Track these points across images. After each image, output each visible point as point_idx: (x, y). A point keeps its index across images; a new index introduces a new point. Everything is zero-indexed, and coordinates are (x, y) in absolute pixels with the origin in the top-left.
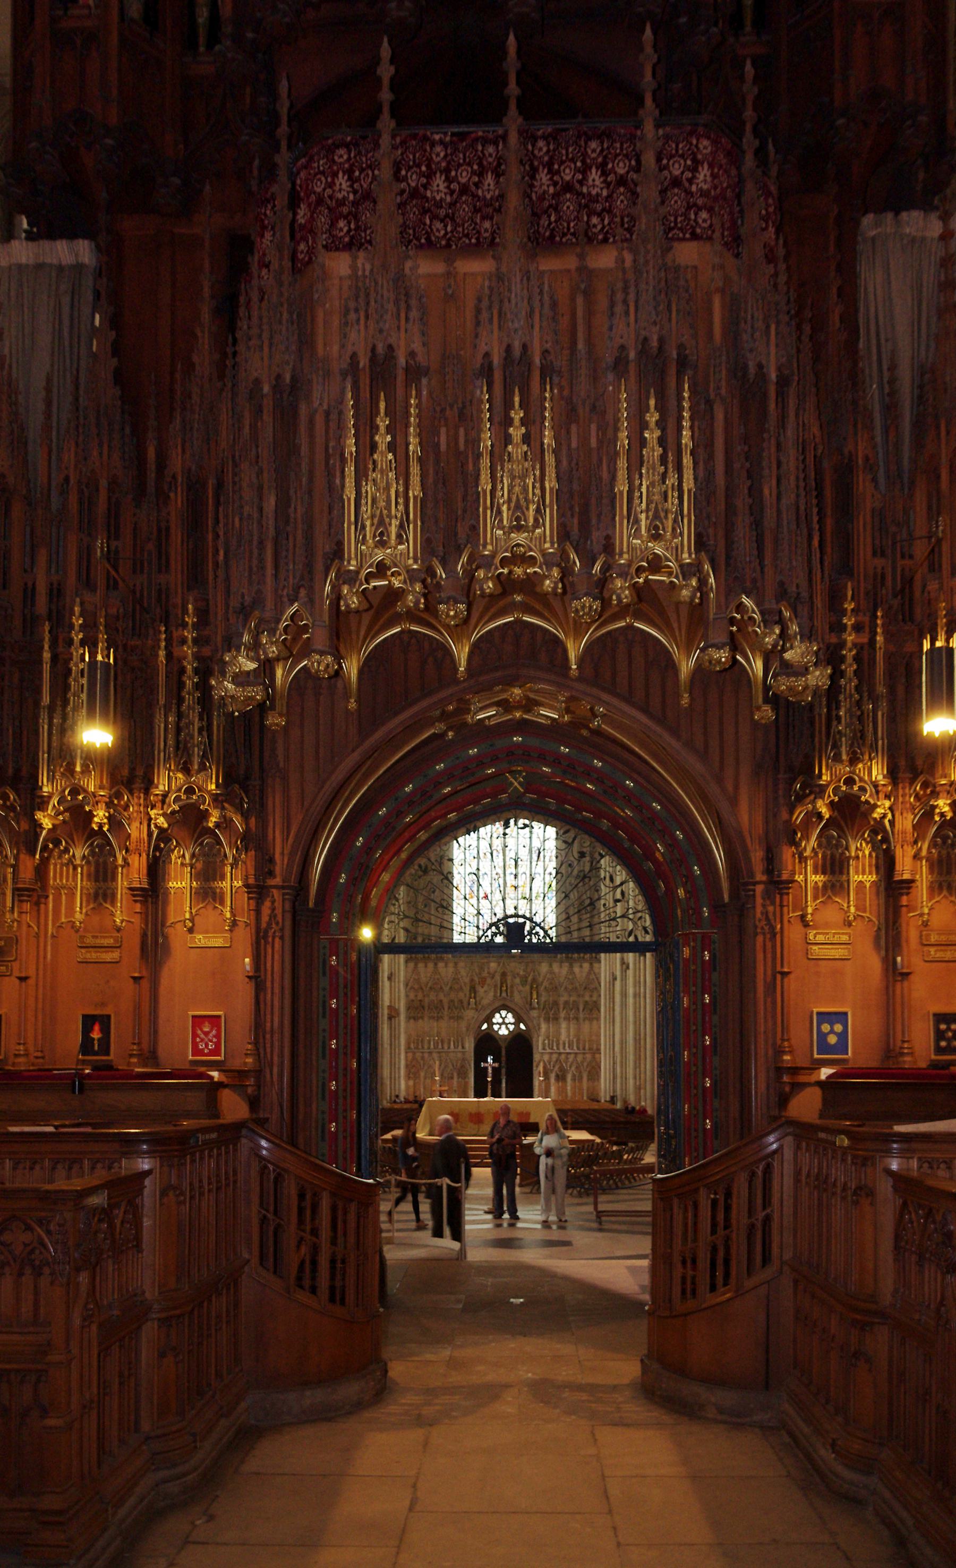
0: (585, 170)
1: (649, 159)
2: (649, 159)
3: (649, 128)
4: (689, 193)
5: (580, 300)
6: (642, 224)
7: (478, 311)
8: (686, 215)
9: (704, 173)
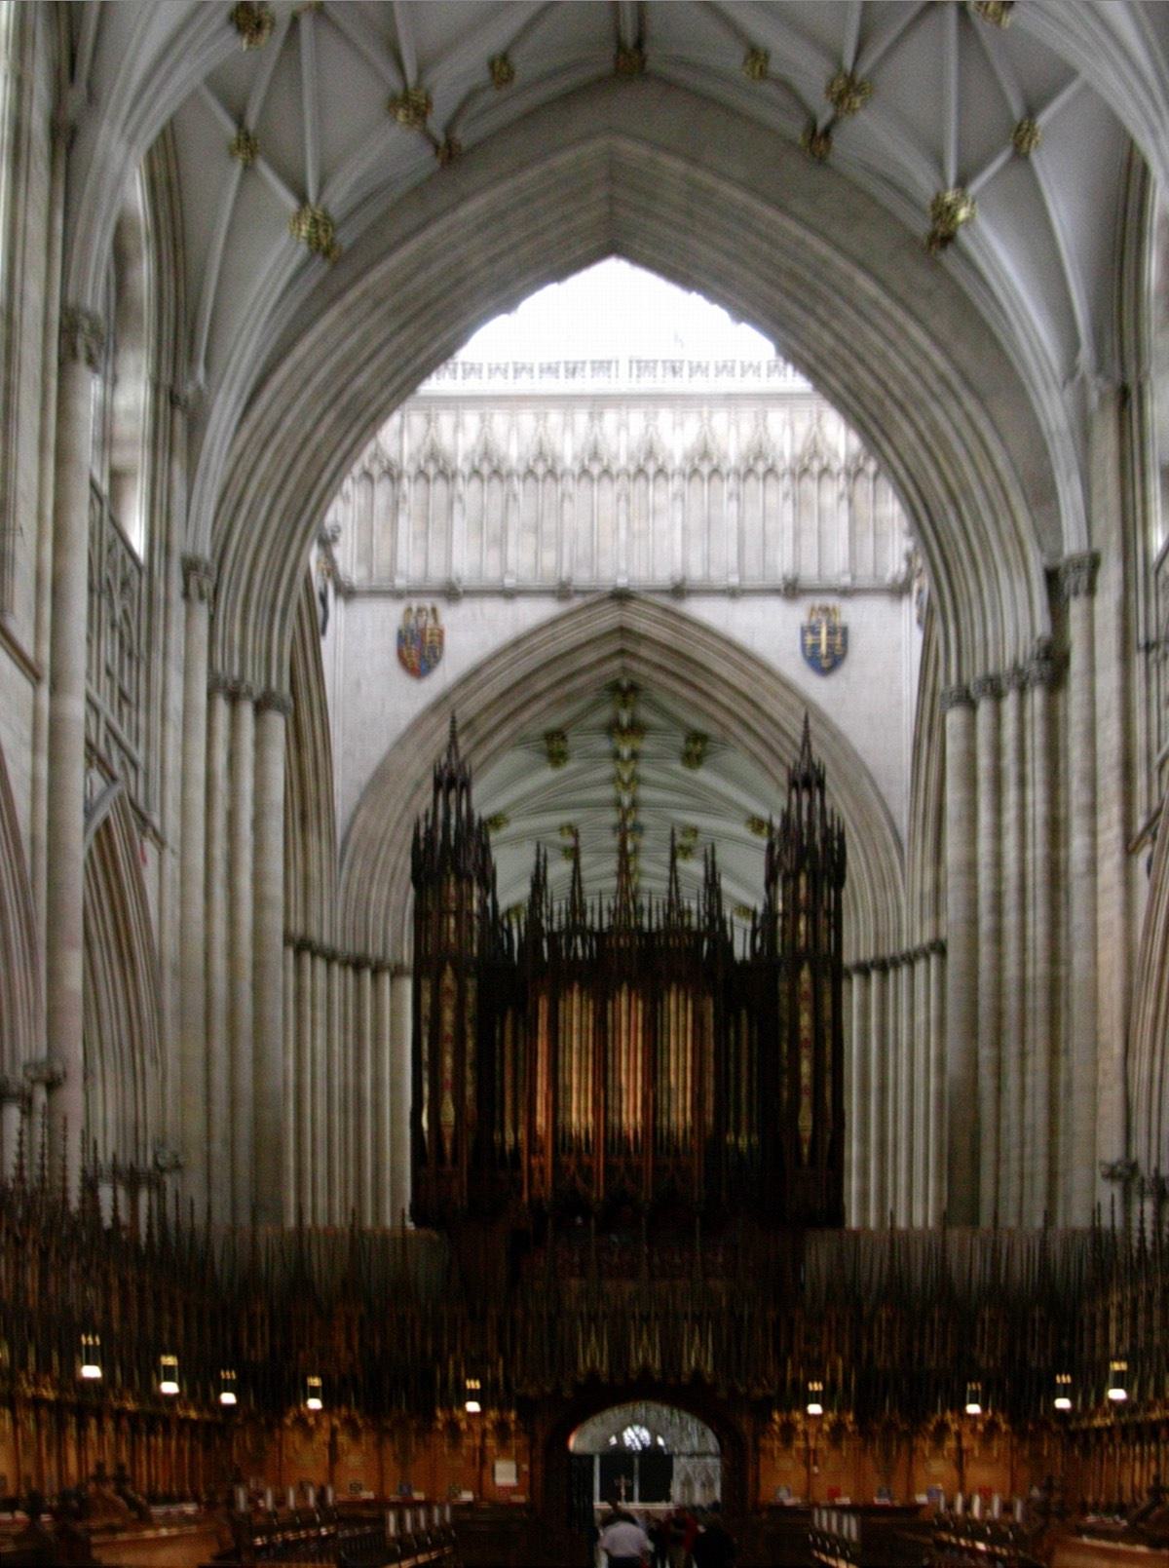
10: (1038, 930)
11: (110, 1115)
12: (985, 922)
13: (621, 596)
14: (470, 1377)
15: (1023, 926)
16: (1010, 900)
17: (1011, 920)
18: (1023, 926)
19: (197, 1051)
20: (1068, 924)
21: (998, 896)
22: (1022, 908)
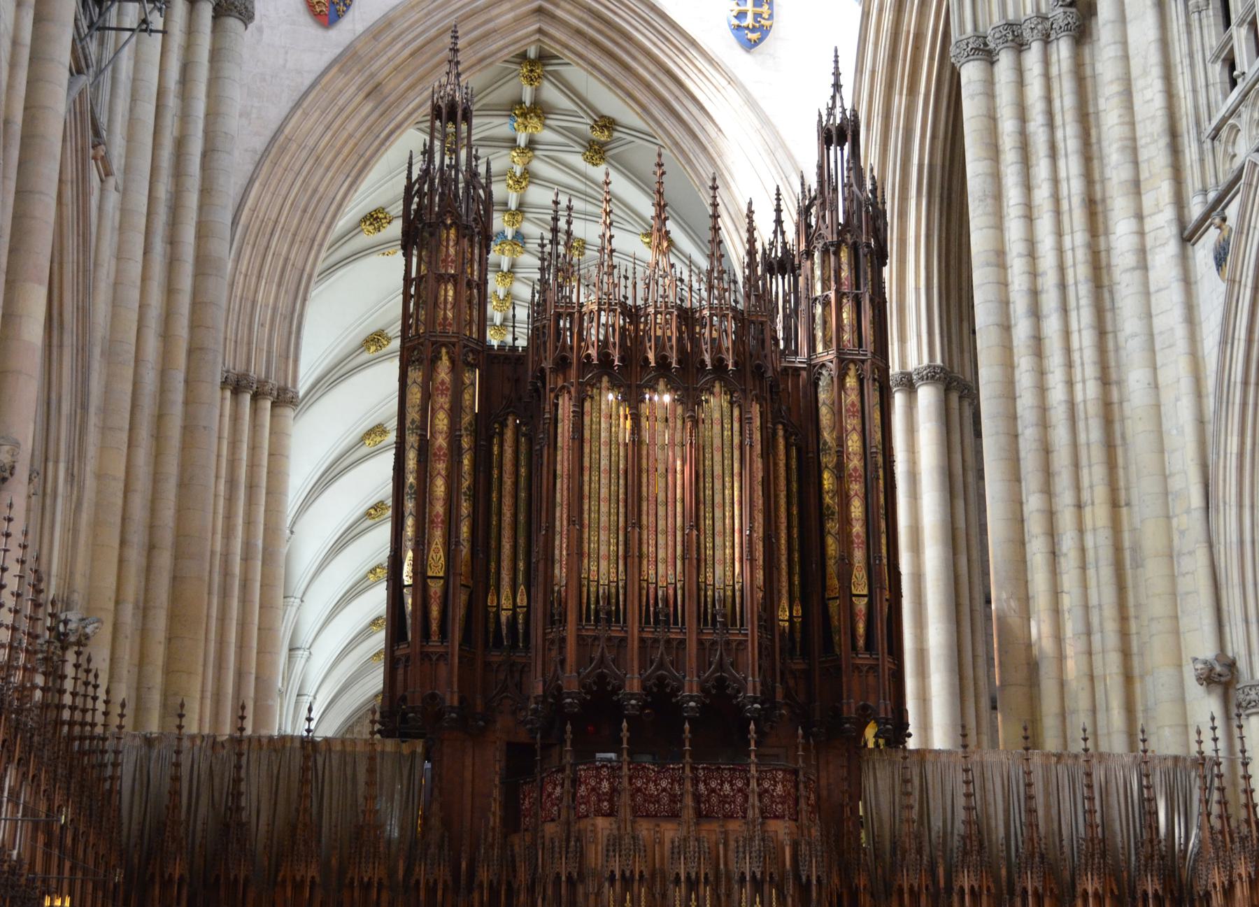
0: (722, 785)
1: (753, 784)
2: (753, 784)
3: (753, 769)
4: (772, 796)
5: (721, 846)
6: (750, 813)
7: (673, 853)
8: (771, 806)
9: (779, 787)
10: (1084, 340)
12: (1022, 330)
15: (1066, 334)
16: (1050, 300)
17: (1052, 326)
18: (1066, 334)
19: (118, 468)
20: (1115, 332)
21: (1034, 294)
22: (1064, 310)
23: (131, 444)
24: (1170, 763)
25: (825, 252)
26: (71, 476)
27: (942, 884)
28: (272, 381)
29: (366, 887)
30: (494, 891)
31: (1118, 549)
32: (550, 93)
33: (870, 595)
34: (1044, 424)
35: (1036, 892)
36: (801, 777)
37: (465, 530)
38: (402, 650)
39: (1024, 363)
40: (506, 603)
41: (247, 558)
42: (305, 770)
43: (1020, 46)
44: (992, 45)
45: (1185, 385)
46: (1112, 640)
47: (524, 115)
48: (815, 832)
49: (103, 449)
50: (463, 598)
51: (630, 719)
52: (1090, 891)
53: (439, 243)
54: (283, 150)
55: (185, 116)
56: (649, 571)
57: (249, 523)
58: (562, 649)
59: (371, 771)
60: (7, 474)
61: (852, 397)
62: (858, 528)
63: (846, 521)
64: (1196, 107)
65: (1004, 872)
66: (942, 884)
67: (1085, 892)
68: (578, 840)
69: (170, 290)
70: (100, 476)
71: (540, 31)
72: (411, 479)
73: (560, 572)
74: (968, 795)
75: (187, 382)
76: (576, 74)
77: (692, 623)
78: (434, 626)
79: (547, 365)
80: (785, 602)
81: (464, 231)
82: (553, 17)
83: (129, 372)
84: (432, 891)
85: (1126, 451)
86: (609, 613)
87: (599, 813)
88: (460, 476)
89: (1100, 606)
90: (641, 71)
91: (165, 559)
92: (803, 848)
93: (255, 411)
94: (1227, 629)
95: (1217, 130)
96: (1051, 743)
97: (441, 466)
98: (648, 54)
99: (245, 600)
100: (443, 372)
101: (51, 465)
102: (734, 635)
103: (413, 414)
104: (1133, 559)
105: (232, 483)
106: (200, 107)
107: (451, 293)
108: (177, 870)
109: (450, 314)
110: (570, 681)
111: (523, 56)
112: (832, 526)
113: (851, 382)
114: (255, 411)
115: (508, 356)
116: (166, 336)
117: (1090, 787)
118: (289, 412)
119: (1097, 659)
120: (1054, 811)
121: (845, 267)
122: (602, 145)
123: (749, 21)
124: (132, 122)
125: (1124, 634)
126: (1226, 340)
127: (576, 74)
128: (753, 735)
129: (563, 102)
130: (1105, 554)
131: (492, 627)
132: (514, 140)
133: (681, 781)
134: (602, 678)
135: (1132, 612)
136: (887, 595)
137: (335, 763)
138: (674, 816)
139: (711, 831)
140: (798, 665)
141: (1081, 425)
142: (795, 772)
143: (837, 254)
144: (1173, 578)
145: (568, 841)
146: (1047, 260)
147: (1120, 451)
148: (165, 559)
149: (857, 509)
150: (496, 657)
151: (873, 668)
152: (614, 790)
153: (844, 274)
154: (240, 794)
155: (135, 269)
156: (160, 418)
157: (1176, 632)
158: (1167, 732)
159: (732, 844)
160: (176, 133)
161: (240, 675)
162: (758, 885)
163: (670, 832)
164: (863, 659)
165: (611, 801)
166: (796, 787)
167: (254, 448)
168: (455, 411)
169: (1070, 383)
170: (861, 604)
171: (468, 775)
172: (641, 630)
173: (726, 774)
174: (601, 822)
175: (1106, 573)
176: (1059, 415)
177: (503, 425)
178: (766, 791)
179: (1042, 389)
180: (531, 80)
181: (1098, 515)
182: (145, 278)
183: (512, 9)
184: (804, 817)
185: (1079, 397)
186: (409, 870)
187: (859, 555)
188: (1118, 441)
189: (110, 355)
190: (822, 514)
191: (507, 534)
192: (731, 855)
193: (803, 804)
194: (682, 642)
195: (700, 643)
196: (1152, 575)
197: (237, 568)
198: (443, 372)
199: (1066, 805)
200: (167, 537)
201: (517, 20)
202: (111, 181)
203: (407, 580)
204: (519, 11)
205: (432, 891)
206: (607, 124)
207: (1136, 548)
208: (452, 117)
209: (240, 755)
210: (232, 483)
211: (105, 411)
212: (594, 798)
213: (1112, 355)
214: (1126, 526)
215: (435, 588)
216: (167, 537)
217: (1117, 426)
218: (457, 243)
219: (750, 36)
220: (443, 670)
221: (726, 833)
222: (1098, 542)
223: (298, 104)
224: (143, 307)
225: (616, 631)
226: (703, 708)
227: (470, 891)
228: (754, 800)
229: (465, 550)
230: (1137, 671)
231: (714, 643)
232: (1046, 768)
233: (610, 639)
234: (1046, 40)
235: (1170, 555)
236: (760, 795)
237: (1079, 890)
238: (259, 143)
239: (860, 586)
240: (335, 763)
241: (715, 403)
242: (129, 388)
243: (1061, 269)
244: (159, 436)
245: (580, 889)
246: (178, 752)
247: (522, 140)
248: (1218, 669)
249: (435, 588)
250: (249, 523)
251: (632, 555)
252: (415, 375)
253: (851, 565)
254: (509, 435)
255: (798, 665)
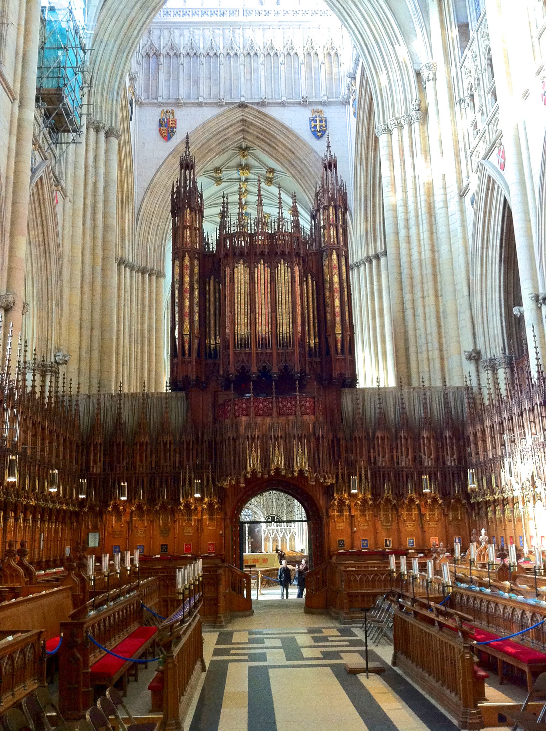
1: (298, 403)
2: (298, 403)
6: (297, 414)
11: (35, 336)
13: (242, 106)
14: (196, 478)
16: (412, 222)
17: (413, 231)
19: (77, 301)
20: (436, 233)
21: (407, 220)
23: (82, 293)
24: (456, 389)
25: (324, 209)
26: (57, 305)
27: (371, 435)
28: (155, 269)
29: (165, 444)
30: (210, 444)
31: (438, 312)
32: (252, 161)
33: (342, 333)
34: (411, 268)
35: (405, 437)
36: (316, 399)
37: (196, 317)
38: (176, 360)
39: (403, 245)
40: (213, 342)
41: (150, 331)
42: (143, 404)
43: (401, 127)
44: (390, 128)
45: (461, 250)
46: (436, 346)
47: (242, 169)
48: (321, 419)
49: (71, 295)
50: (197, 341)
51: (253, 382)
52: (425, 436)
53: (183, 214)
54: (154, 187)
55: (96, 174)
56: (259, 328)
57: (150, 319)
58: (229, 357)
59: (166, 403)
60: (12, 305)
61: (335, 262)
62: (338, 310)
63: (334, 307)
64: (465, 145)
65: (393, 431)
66: (371, 435)
67: (423, 437)
68: (236, 425)
69: (94, 237)
70: (70, 305)
71: (244, 138)
72: (177, 300)
73: (228, 330)
74: (380, 404)
75: (103, 270)
76: (259, 153)
77: (274, 347)
78: (187, 352)
79: (221, 256)
80: (312, 337)
81: (192, 209)
82: (248, 132)
83: (79, 267)
84: (188, 444)
85: (441, 276)
86: (245, 344)
87: (243, 415)
88: (193, 297)
89: (431, 333)
90: (280, 150)
91: (97, 333)
92: (317, 424)
93: (150, 280)
94: (477, 340)
95: (472, 153)
96: (415, 384)
97: (187, 295)
98: (283, 144)
99: (150, 346)
100: (187, 261)
101: (50, 301)
102: (290, 350)
103: (177, 277)
104: (444, 315)
105: (143, 305)
106: (102, 171)
107: (188, 233)
108: (99, 440)
109: (188, 240)
110: (232, 369)
111: (240, 148)
112: (329, 309)
113: (335, 256)
114: (150, 280)
115: (211, 255)
116: (93, 254)
117: (425, 399)
118: (162, 279)
119: (430, 353)
120: (412, 408)
121: (331, 214)
122: (271, 178)
123: (318, 128)
124: (75, 177)
125: (440, 343)
126: (475, 232)
127: (259, 153)
128: (297, 385)
129: (257, 164)
130: (433, 314)
131: (208, 351)
132: (240, 179)
133: (272, 403)
134: (243, 367)
135: (443, 335)
136: (349, 333)
137: (155, 401)
138: (270, 415)
139: (282, 419)
140: (317, 359)
141: (424, 267)
142: (314, 398)
143: (328, 210)
144: (458, 322)
145: (232, 425)
146: (411, 207)
147: (438, 276)
148: (97, 333)
149: (337, 303)
150: (210, 361)
151: (344, 360)
152: (248, 407)
153: (331, 217)
154: (121, 413)
155: (80, 230)
156: (93, 283)
157: (459, 342)
158: (456, 378)
159: (291, 424)
160: (93, 181)
161: (149, 371)
162: (300, 438)
163: (268, 420)
164: (340, 357)
165: (246, 411)
166: (314, 403)
167: (150, 293)
168: (191, 276)
169: (420, 252)
170: (339, 337)
171: (201, 403)
172: (257, 349)
173: (289, 400)
174: (244, 418)
175: (434, 321)
176: (416, 264)
177: (210, 279)
178: (303, 405)
179: (410, 255)
180: (244, 156)
181: (430, 300)
182: (84, 233)
183: (233, 130)
184: (317, 414)
185: (423, 257)
186: (181, 437)
187: (338, 319)
188: (438, 273)
189: (72, 261)
190: (325, 305)
191: (212, 318)
192: (290, 428)
193: (317, 409)
194: (271, 353)
195: (278, 353)
196: (450, 322)
197: (146, 335)
198: (187, 261)
199: (417, 406)
200: (97, 325)
201: (235, 134)
202: (67, 199)
203: (177, 336)
204: (235, 131)
205: (188, 444)
206: (272, 171)
207: (445, 312)
208: (187, 167)
209: (120, 400)
210: (143, 305)
211: (71, 280)
212: (240, 410)
213: (435, 241)
214: (441, 304)
215: (187, 338)
216: (97, 325)
217: (437, 267)
218: (190, 214)
219: (319, 134)
220: (189, 367)
221: (288, 420)
222: (431, 310)
223: (158, 170)
224: (83, 244)
225: (247, 351)
226: (279, 377)
227: (202, 443)
228: (298, 408)
229: (197, 324)
230: (445, 356)
231: (283, 353)
232: (409, 393)
233: (245, 353)
234: (410, 124)
235: (457, 314)
236: (301, 407)
237: (421, 436)
238: (146, 185)
239: (338, 330)
240: (155, 401)
241: (282, 268)
242: (79, 273)
243: (416, 210)
244: (92, 289)
245: (237, 441)
246: (98, 400)
247: (243, 179)
248: (473, 355)
249: (187, 338)
250: (150, 319)
251: (252, 323)
252: (177, 263)
253: (335, 323)
254: (212, 282)
255: (317, 359)
